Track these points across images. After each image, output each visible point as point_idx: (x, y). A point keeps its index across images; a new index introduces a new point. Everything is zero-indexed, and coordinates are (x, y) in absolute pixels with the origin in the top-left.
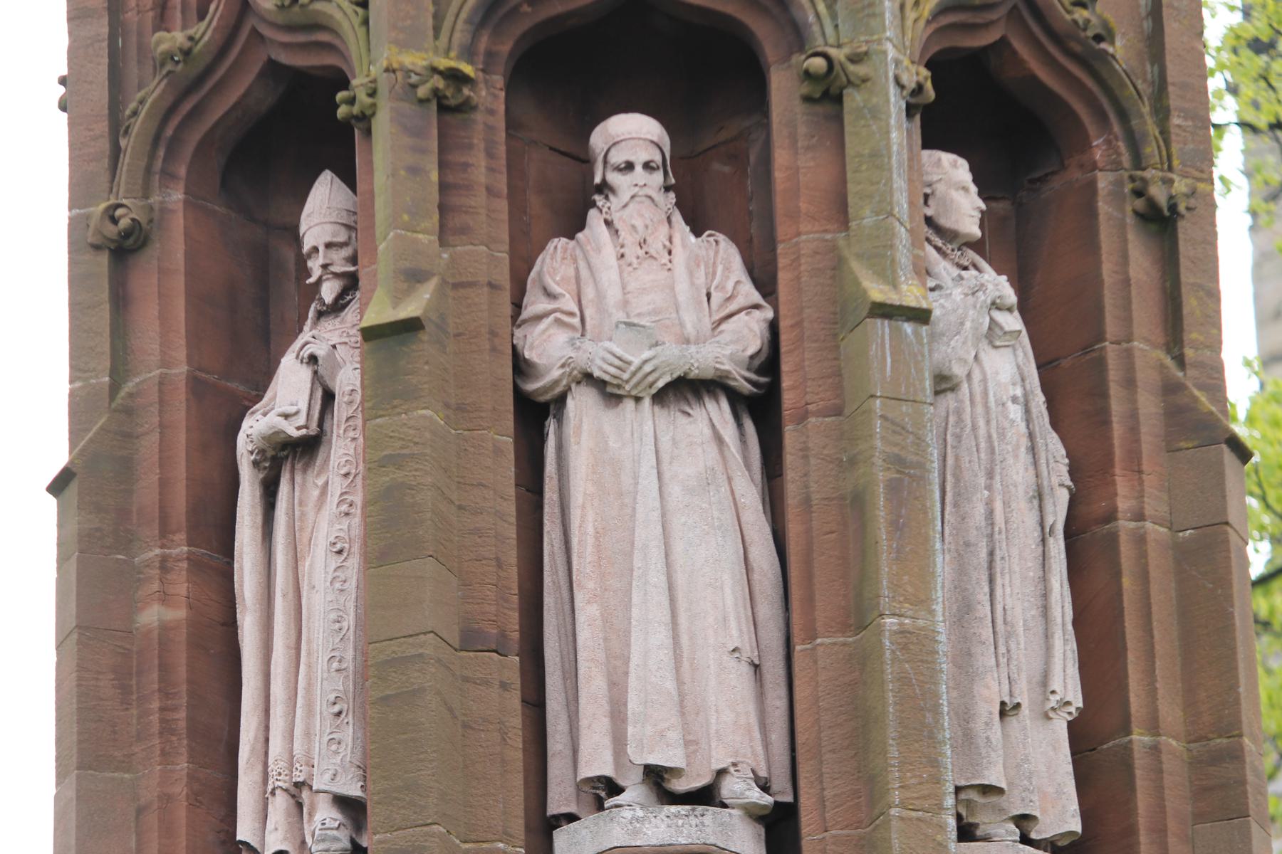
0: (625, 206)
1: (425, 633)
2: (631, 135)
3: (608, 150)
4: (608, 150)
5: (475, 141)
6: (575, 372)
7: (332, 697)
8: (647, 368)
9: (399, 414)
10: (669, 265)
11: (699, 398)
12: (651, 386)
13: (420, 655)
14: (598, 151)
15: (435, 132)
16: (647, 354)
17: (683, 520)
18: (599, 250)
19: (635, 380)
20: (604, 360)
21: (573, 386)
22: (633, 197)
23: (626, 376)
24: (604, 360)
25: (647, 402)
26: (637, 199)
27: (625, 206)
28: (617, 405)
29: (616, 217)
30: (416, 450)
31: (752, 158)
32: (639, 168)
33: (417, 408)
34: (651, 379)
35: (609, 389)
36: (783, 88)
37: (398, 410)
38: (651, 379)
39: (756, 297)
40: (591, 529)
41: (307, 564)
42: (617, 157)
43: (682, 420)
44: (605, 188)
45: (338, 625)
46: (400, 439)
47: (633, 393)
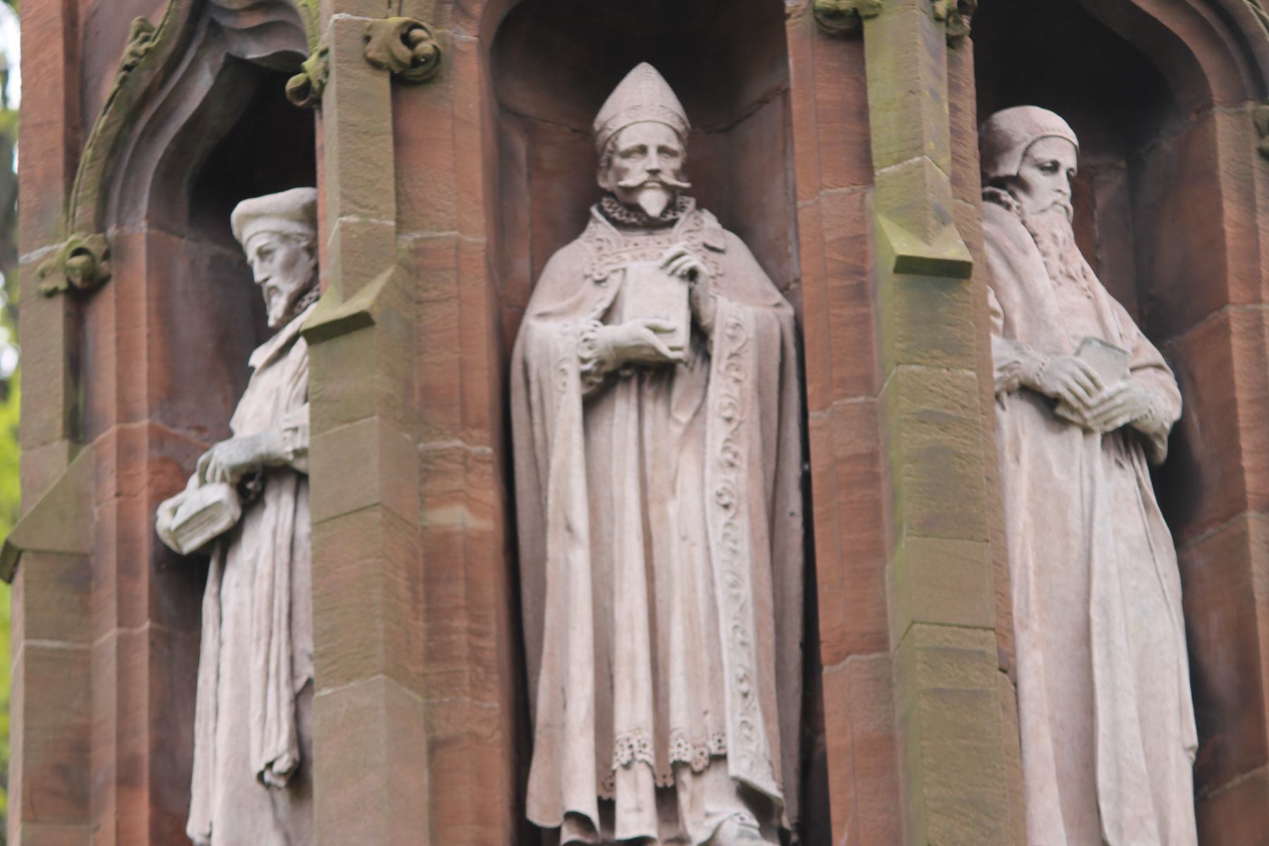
0: (1043, 211)
1: (985, 629)
2: (1044, 134)
3: (1034, 142)
4: (1034, 142)
5: (963, 84)
6: (1016, 381)
7: (741, 672)
8: (1119, 400)
9: (940, 367)
10: (1090, 293)
11: (1128, 451)
12: (1106, 423)
13: (982, 653)
14: (1016, 139)
15: (945, 59)
16: (1122, 384)
17: (1133, 583)
18: (1025, 252)
19: (1101, 409)
20: (1073, 376)
21: (1004, 396)
22: (1055, 203)
23: (1091, 402)
24: (1073, 376)
25: (1098, 438)
26: (1058, 207)
27: (1043, 211)
28: (1060, 431)
29: (1031, 219)
30: (962, 414)
31: (1101, 199)
32: (1062, 173)
33: (962, 367)
34: (1114, 413)
35: (1060, 411)
36: (1228, 134)
37: (939, 362)
38: (1114, 413)
39: (1158, 357)
40: (1031, 564)
41: (672, 508)
42: (1045, 153)
43: (1116, 471)
44: (1018, 183)
45: (734, 591)
46: (945, 396)
47: (1090, 424)
